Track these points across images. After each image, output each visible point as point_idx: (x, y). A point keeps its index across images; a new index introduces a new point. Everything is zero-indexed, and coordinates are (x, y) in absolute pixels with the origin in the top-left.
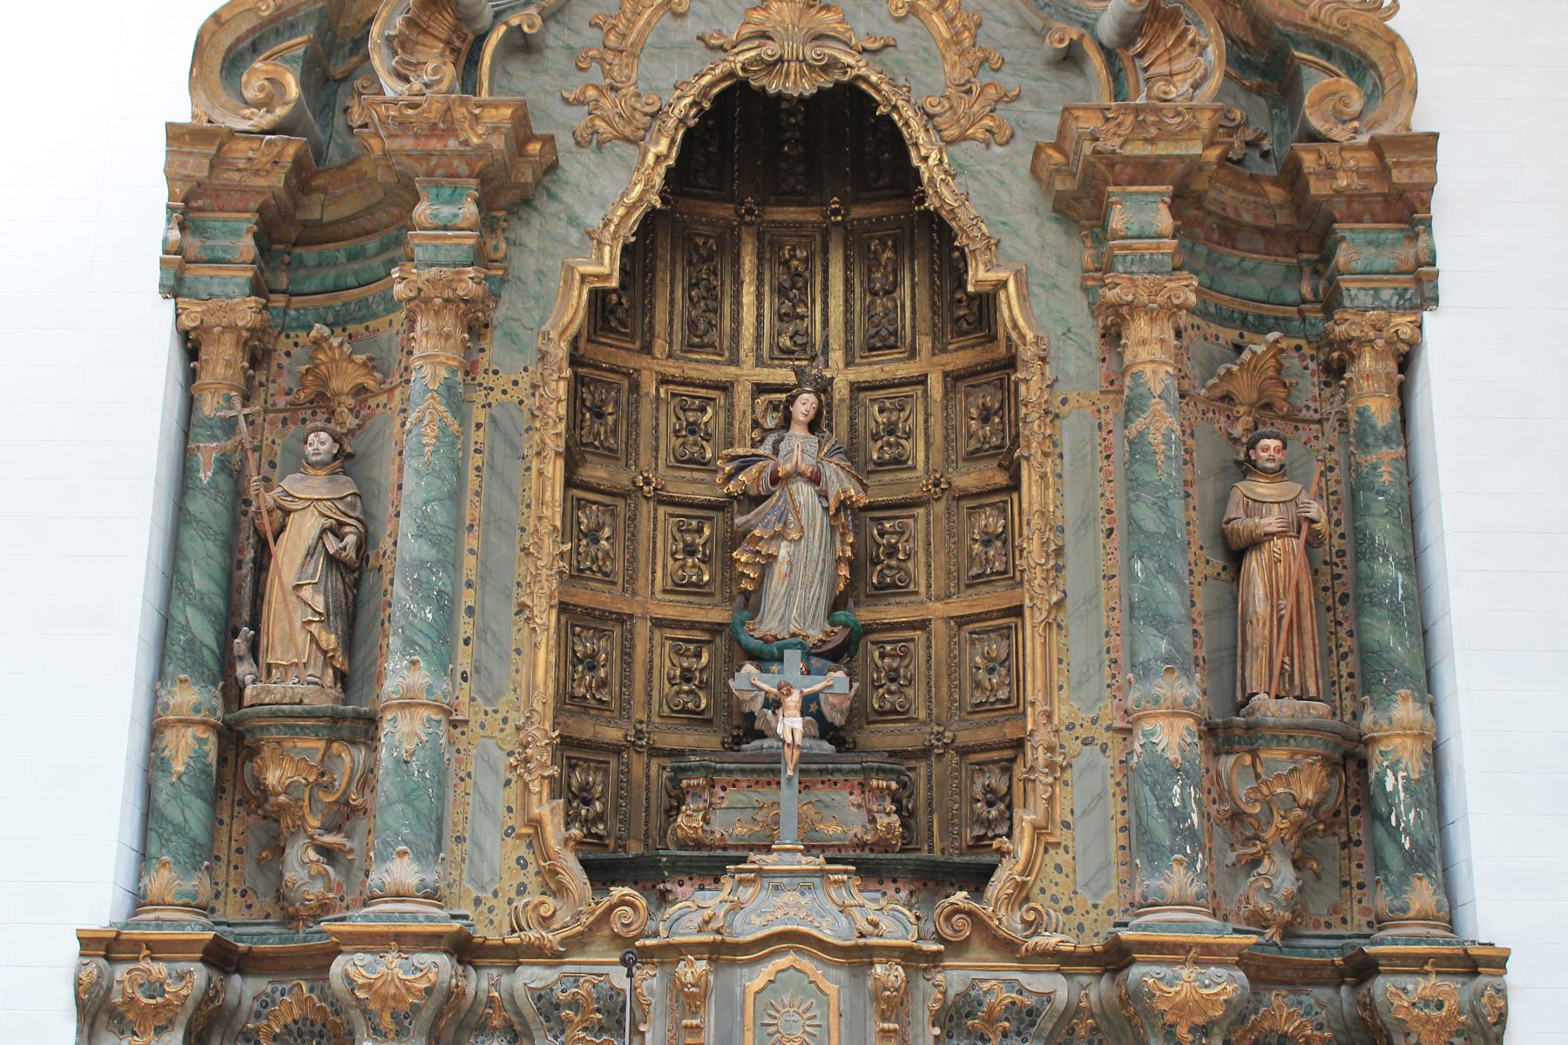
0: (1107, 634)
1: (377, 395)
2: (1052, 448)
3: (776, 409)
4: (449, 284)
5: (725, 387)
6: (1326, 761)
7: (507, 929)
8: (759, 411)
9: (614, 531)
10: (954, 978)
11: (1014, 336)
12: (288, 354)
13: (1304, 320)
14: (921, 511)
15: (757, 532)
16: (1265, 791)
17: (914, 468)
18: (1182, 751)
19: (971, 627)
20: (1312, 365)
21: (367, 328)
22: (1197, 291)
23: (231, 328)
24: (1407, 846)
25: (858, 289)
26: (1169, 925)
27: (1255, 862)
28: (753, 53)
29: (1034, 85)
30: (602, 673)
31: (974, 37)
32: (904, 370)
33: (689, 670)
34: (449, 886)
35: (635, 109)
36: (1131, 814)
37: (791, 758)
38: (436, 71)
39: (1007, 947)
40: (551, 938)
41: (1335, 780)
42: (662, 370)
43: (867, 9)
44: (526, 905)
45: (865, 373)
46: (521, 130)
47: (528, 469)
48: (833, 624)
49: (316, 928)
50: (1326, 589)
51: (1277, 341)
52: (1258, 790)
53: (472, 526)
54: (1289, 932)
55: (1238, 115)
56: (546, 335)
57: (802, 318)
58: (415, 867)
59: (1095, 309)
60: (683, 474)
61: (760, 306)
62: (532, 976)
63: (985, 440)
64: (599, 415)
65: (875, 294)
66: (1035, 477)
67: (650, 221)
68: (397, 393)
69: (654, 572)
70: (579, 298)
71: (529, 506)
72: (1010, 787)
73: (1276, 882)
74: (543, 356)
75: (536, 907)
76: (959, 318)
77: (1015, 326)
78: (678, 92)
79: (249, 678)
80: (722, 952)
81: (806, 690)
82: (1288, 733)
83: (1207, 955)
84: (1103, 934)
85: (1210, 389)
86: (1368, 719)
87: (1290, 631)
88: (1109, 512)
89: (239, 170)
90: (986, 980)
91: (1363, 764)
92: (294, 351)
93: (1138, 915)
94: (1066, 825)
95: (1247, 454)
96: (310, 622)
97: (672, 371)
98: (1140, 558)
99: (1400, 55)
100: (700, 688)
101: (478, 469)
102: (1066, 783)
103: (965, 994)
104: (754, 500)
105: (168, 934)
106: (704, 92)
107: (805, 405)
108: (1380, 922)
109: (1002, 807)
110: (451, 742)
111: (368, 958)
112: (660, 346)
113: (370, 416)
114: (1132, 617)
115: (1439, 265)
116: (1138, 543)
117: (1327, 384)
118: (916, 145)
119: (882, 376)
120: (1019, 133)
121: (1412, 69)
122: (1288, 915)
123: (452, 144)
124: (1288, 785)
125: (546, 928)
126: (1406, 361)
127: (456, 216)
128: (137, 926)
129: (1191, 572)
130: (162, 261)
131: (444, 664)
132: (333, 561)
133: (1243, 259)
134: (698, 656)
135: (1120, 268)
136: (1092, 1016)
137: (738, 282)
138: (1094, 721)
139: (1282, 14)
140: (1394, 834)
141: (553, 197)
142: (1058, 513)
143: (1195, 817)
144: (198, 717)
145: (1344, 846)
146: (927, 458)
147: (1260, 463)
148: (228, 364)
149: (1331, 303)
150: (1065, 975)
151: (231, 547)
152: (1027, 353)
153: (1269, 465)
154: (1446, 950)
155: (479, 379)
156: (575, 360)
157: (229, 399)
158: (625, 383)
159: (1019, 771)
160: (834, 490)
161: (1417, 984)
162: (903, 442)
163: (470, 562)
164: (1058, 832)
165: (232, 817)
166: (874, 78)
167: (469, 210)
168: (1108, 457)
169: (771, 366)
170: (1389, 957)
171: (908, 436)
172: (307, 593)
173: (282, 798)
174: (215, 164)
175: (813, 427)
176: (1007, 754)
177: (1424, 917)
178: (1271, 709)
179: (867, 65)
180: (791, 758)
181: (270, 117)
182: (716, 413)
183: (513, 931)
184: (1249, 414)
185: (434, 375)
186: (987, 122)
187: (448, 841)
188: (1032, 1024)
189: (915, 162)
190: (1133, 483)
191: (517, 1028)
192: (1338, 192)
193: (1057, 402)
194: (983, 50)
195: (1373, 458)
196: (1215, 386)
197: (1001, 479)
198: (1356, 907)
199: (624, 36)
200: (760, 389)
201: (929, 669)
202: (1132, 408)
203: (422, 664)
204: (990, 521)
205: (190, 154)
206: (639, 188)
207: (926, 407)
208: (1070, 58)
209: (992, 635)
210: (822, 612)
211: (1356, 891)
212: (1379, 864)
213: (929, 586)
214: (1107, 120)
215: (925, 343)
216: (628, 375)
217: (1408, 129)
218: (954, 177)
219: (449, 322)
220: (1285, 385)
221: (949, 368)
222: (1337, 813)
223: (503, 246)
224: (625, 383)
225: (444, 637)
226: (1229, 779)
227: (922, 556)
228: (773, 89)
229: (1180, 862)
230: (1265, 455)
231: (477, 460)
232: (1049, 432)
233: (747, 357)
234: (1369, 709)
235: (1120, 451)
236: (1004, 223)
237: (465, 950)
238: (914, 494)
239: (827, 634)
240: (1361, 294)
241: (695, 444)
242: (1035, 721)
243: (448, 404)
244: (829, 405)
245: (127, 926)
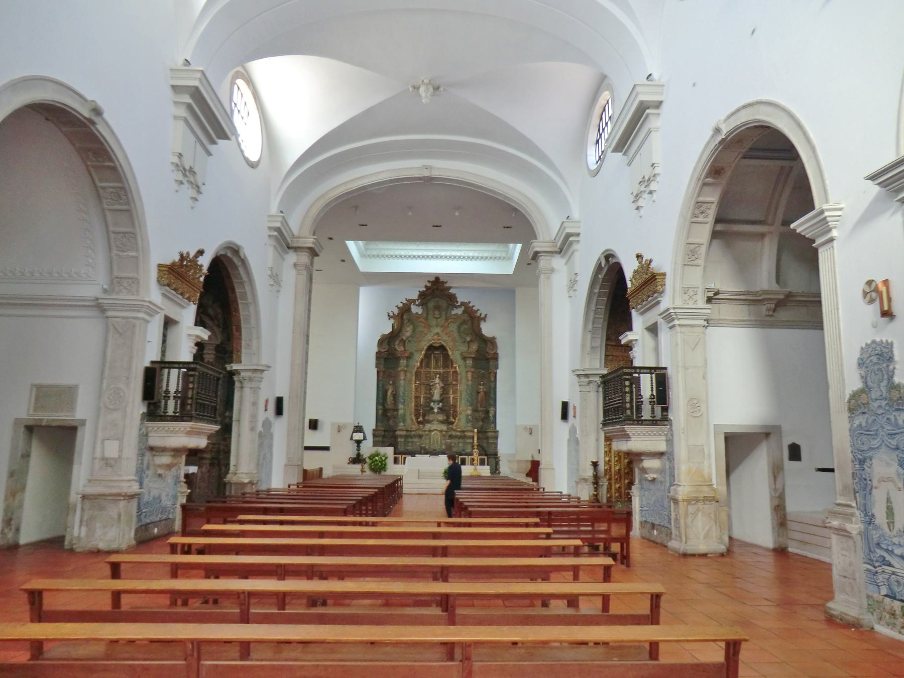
2: (461, 383)
10: (450, 433)
39: (454, 430)
45: (445, 370)
62: (413, 433)
70: (416, 368)
80: (430, 431)
82: (481, 411)
107: (438, 376)
126: (496, 374)
202: (468, 381)
208: (464, 342)
225: (404, 402)
237: (407, 431)
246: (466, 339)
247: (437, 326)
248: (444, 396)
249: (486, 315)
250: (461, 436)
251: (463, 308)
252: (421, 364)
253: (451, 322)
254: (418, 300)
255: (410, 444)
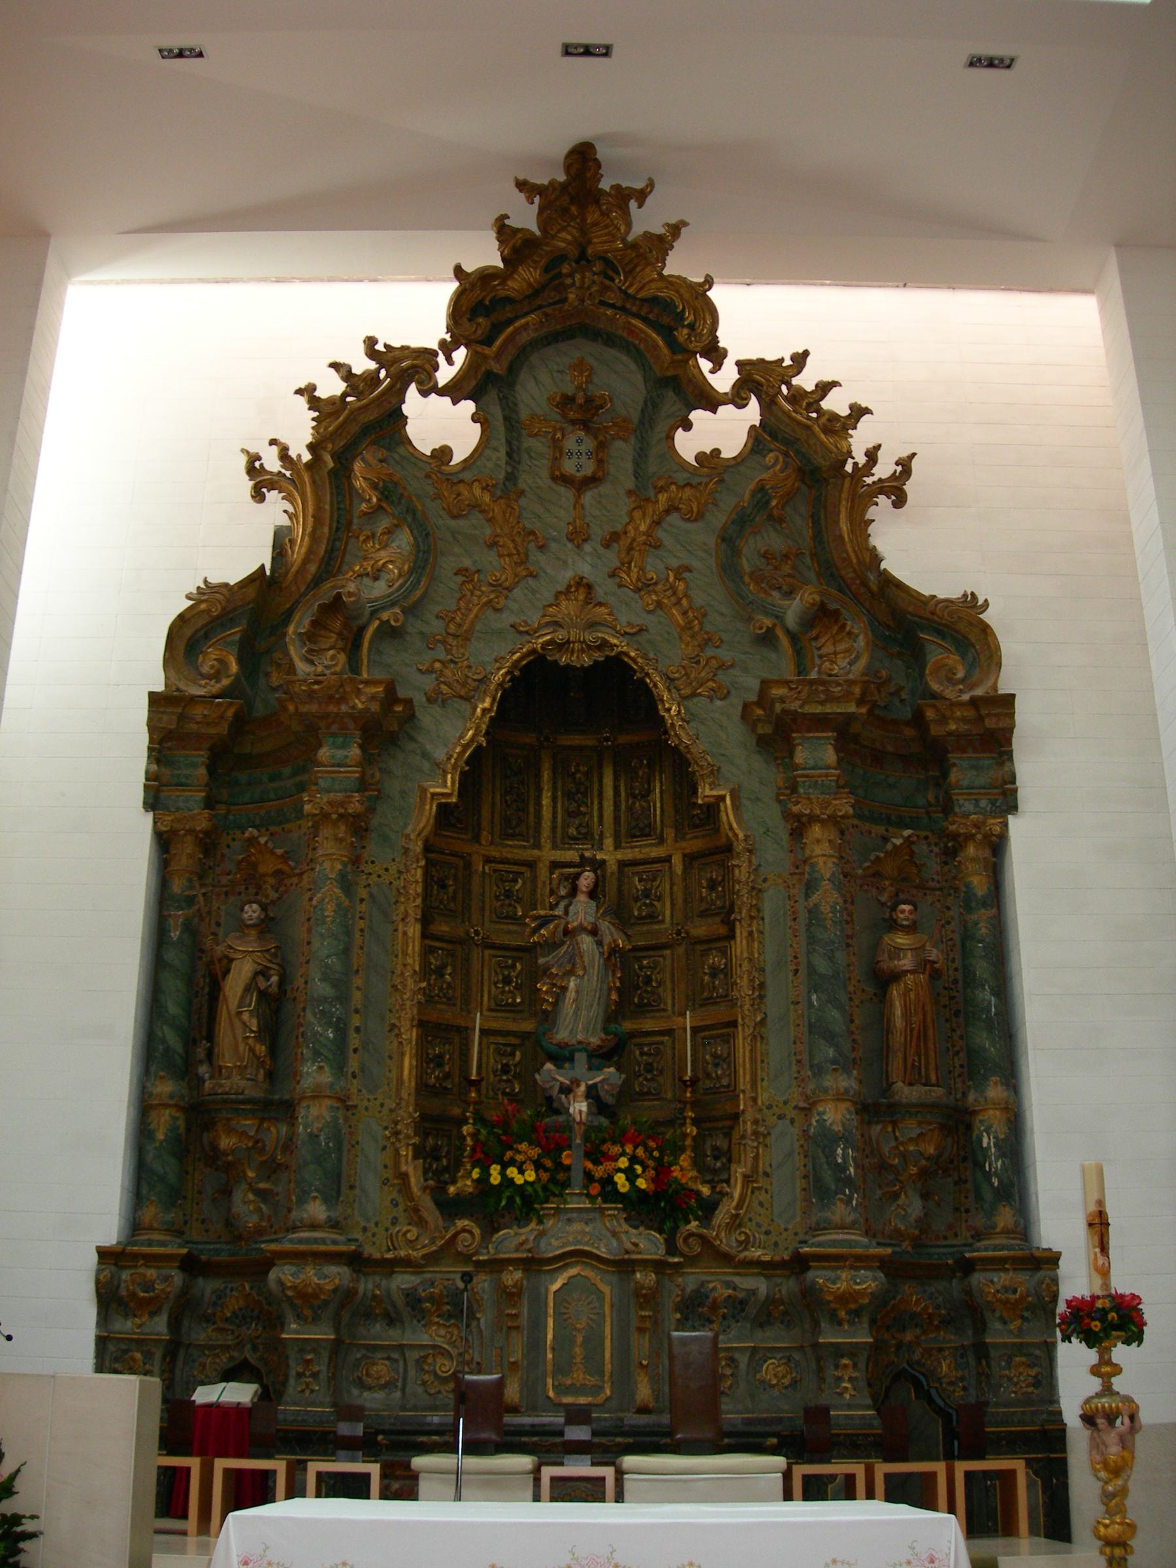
0: (795, 1043)
1: (290, 876)
2: (756, 914)
3: (567, 879)
4: (342, 804)
5: (531, 865)
6: (942, 1127)
7: (384, 1248)
8: (555, 883)
9: (454, 970)
10: (690, 1280)
11: (730, 834)
12: (228, 846)
13: (930, 818)
14: (667, 952)
15: (554, 971)
16: (902, 1148)
17: (663, 921)
18: (843, 1125)
19: (703, 1034)
20: (936, 849)
21: (283, 829)
22: (853, 806)
23: (191, 831)
24: (996, 1184)
25: (623, 794)
26: (834, 1243)
27: (896, 1196)
28: (548, 637)
29: (743, 657)
30: (447, 1069)
31: (701, 624)
32: (655, 852)
33: (507, 1065)
34: (345, 1219)
35: (467, 677)
36: (810, 1167)
37: (579, 1131)
38: (333, 658)
39: (726, 1258)
40: (416, 1254)
41: (950, 1140)
42: (486, 853)
43: (627, 604)
44: (398, 1232)
46: (391, 696)
47: (396, 930)
48: (607, 1033)
49: (254, 1246)
50: (945, 1006)
51: (909, 836)
52: (897, 1148)
53: (358, 971)
54: (917, 1243)
55: (884, 673)
56: (407, 836)
57: (585, 814)
58: (324, 1208)
59: (787, 816)
60: (502, 927)
61: (555, 807)
62: (403, 1281)
63: (713, 903)
64: (443, 886)
65: (634, 797)
66: (745, 934)
67: (477, 758)
68: (305, 876)
69: (482, 996)
70: (431, 809)
71: (397, 956)
72: (730, 1147)
73: (909, 1211)
74: (406, 851)
75: (405, 1234)
76: (694, 816)
77: (731, 828)
78: (498, 665)
79: (207, 1076)
80: (534, 1265)
81: (590, 1082)
83: (859, 1261)
84: (790, 1250)
85: (864, 870)
86: (971, 1097)
87: (919, 1037)
88: (796, 957)
89: (198, 723)
90: (709, 1282)
91: (969, 1127)
92: (232, 844)
93: (814, 1236)
94: (766, 1174)
95: (891, 916)
96: (248, 1037)
97: (494, 853)
98: (816, 992)
99: (990, 639)
100: (514, 1077)
101: (362, 930)
102: (766, 1146)
103: (697, 1292)
104: (552, 945)
105: (156, 1250)
106: (515, 664)
107: (586, 880)
108: (978, 1236)
109: (724, 1160)
110: (346, 1120)
111: (294, 1269)
112: (485, 835)
113: (286, 892)
114: (810, 1032)
115: (1018, 784)
116: (816, 982)
117: (946, 863)
118: (662, 700)
119: (642, 856)
120: (733, 692)
121: (998, 648)
122: (917, 1232)
123: (344, 708)
124: (917, 1145)
125: (415, 1250)
127: (346, 757)
128: (135, 1244)
129: (851, 999)
130: (146, 786)
131: (340, 1068)
132: (263, 995)
133: (887, 776)
134: (513, 1054)
135: (801, 791)
136: (783, 1303)
137: (539, 790)
138: (785, 1103)
139: (910, 609)
140: (988, 1176)
141: (412, 739)
142: (761, 958)
143: (852, 1170)
144: (172, 1102)
145: (956, 1183)
146: (672, 915)
147: (899, 921)
148: (190, 856)
149: (947, 807)
150: (767, 1277)
151: (190, 981)
152: (739, 847)
153: (904, 923)
154: (1019, 1253)
155: (362, 868)
156: (428, 848)
157: (190, 881)
158: (461, 863)
159: (736, 1136)
160: (607, 940)
161: (1000, 1277)
162: (656, 903)
163: (357, 996)
164: (760, 1179)
165: (194, 1170)
166: (632, 654)
167: (355, 752)
168: (795, 919)
169: (562, 849)
170: (983, 1260)
171: (659, 898)
172: (246, 1016)
173: (230, 1158)
174: (182, 717)
175: (592, 894)
176: (728, 1123)
177: (1006, 1232)
178: (906, 1093)
179: (628, 645)
180: (579, 1131)
181: (218, 686)
182: (524, 883)
183: (389, 1250)
184: (891, 885)
185: (332, 867)
186: (711, 684)
187: (344, 1189)
188: (743, 1310)
189: (662, 713)
190: (812, 940)
191: (393, 1315)
192: (950, 734)
193: (760, 881)
194: (707, 633)
195: (974, 917)
196: (868, 867)
197: (723, 930)
198: (964, 1226)
199: (460, 626)
200: (555, 865)
201: (674, 1064)
202: (810, 887)
203: (327, 1069)
204: (714, 959)
205: (163, 713)
206: (471, 733)
207: (671, 879)
208: (767, 639)
209: (718, 1040)
210: (599, 1026)
211: (964, 1215)
212: (979, 1197)
213: (674, 1005)
214: (791, 689)
215: (670, 833)
216: (463, 857)
217: (996, 690)
218: (688, 722)
219: (342, 831)
220: (917, 866)
221: (687, 851)
222: (952, 1162)
223: (378, 774)
224: (461, 863)
226: (878, 1143)
227: (669, 985)
228: (563, 660)
229: (841, 1200)
230: (901, 916)
231: (362, 924)
232: (754, 902)
233: (546, 843)
234: (972, 1091)
235: (803, 916)
236: (723, 755)
237: (356, 1261)
238: (663, 941)
239: (603, 1040)
240: (967, 804)
241: (510, 905)
242: (745, 1104)
243: (342, 888)
244: (604, 876)
245: (128, 1244)
246: (780, 618)
247: (578, 536)
248: (628, 1026)
249: (905, 465)
250: (771, 1300)
251: (752, 412)
252: (469, 782)
253: (672, 509)
254: (447, 348)
255: (381, 1368)
